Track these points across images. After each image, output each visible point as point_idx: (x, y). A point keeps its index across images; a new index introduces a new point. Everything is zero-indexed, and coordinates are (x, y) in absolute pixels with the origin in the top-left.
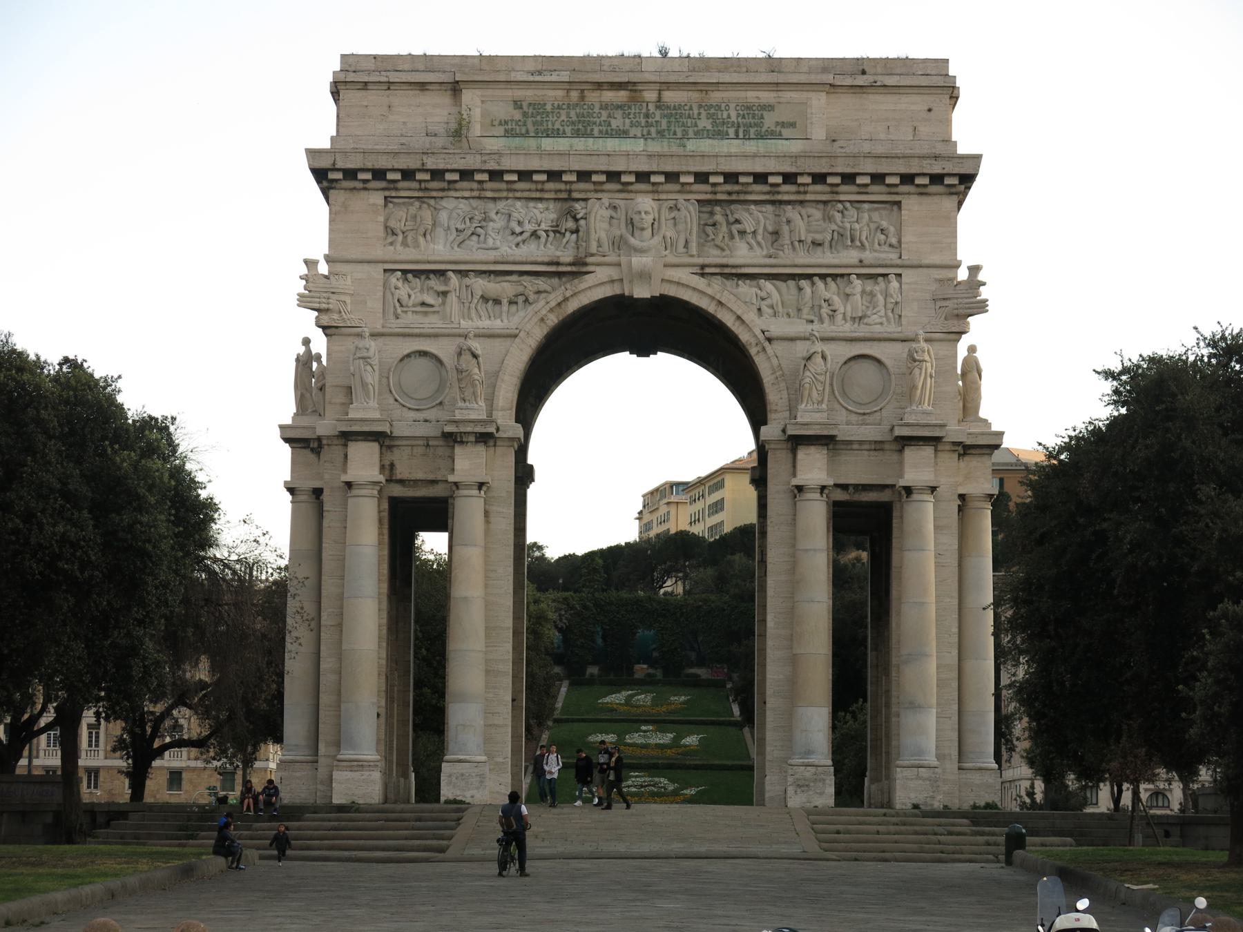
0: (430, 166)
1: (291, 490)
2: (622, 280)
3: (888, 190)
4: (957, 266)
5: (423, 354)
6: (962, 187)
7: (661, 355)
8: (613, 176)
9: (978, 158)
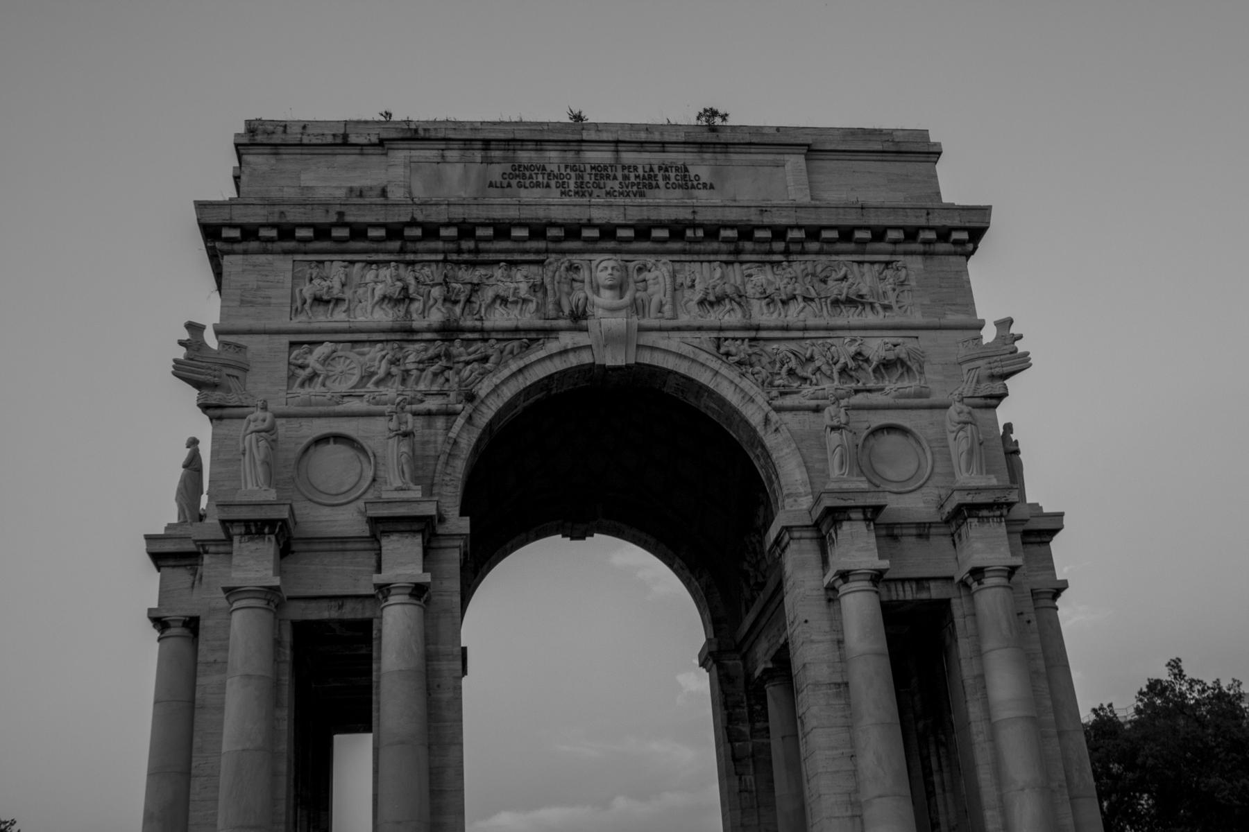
0: (349, 219)
1: (160, 622)
2: (590, 347)
3: (890, 247)
4: (980, 326)
5: (339, 438)
6: (970, 247)
7: (599, 539)
8: (573, 231)
9: (986, 210)
